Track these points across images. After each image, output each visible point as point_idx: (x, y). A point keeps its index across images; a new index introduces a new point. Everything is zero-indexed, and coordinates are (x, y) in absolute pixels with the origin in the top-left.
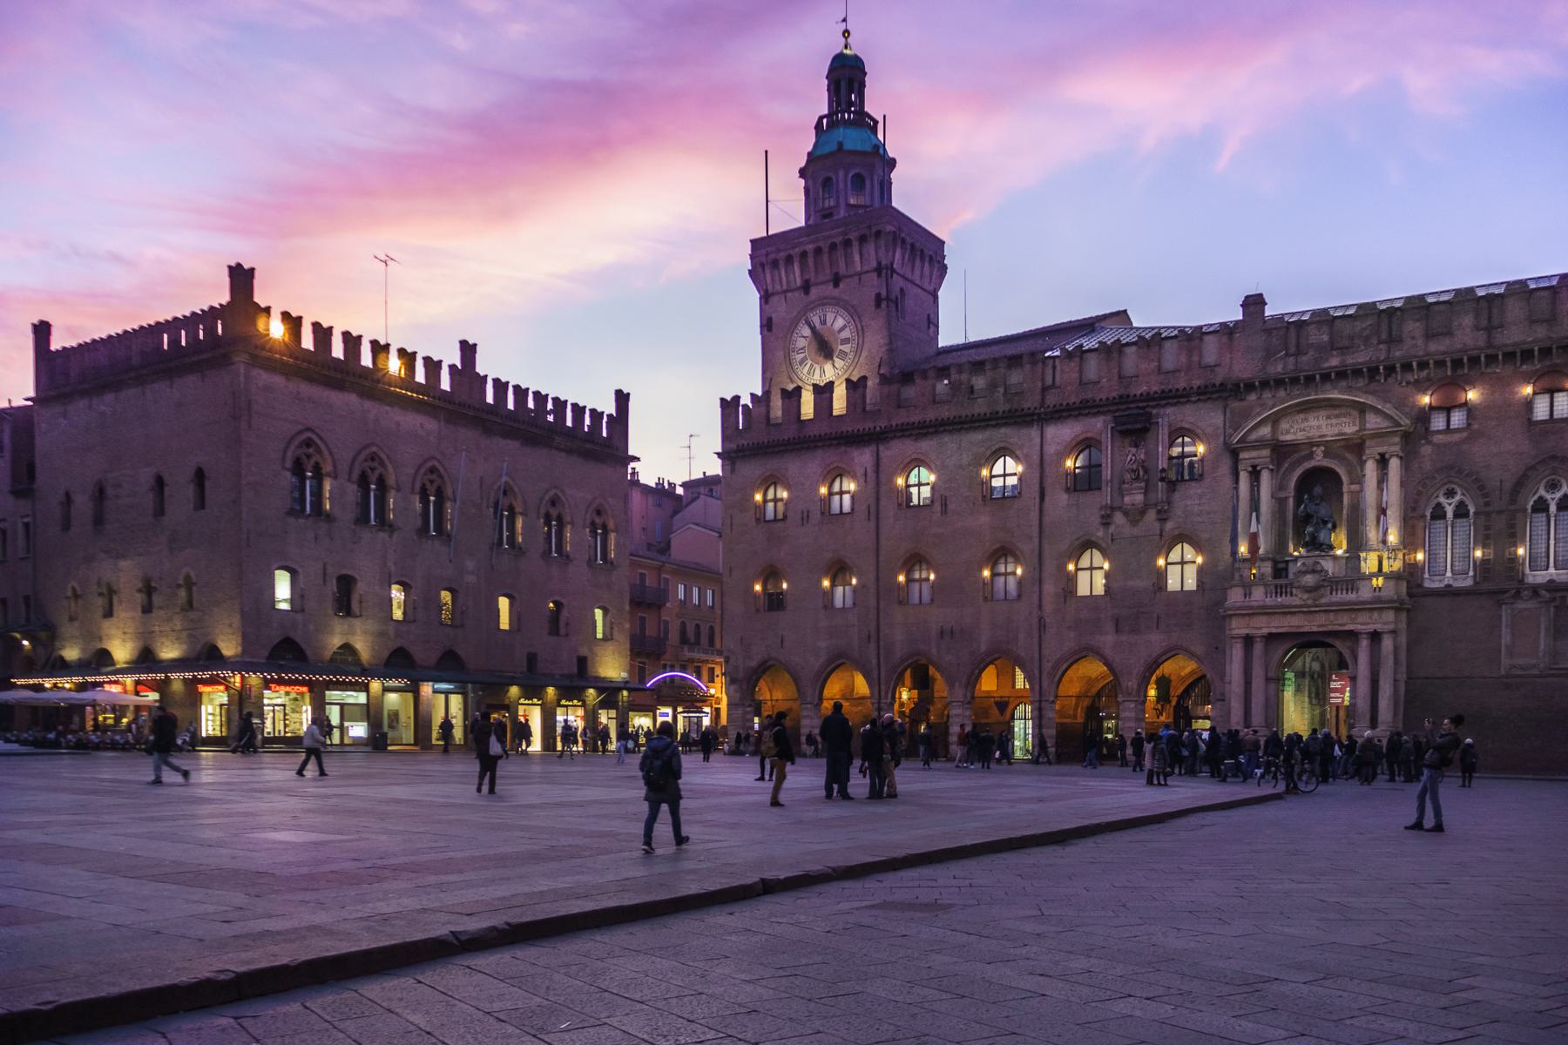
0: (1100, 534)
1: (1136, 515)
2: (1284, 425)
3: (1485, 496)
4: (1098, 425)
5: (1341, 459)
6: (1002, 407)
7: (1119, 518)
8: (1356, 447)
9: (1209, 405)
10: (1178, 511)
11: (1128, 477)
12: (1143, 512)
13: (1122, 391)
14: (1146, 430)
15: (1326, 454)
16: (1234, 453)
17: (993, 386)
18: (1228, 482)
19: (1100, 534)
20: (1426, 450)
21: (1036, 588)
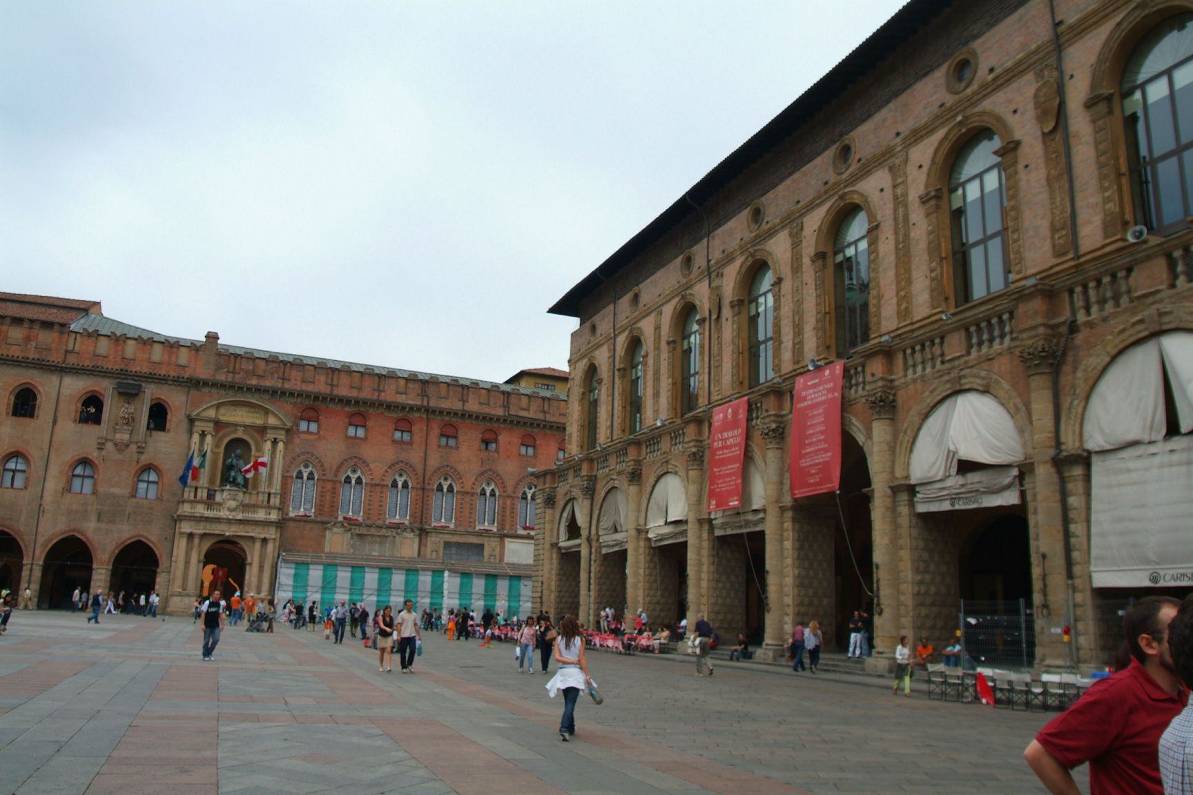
0: (95, 454)
1: (121, 447)
2: (222, 410)
5: (252, 438)
6: (32, 355)
8: (262, 430)
9: (179, 388)
11: (121, 422)
12: (127, 446)
13: (123, 367)
16: (191, 421)
17: (28, 339)
18: (185, 437)
20: (297, 441)
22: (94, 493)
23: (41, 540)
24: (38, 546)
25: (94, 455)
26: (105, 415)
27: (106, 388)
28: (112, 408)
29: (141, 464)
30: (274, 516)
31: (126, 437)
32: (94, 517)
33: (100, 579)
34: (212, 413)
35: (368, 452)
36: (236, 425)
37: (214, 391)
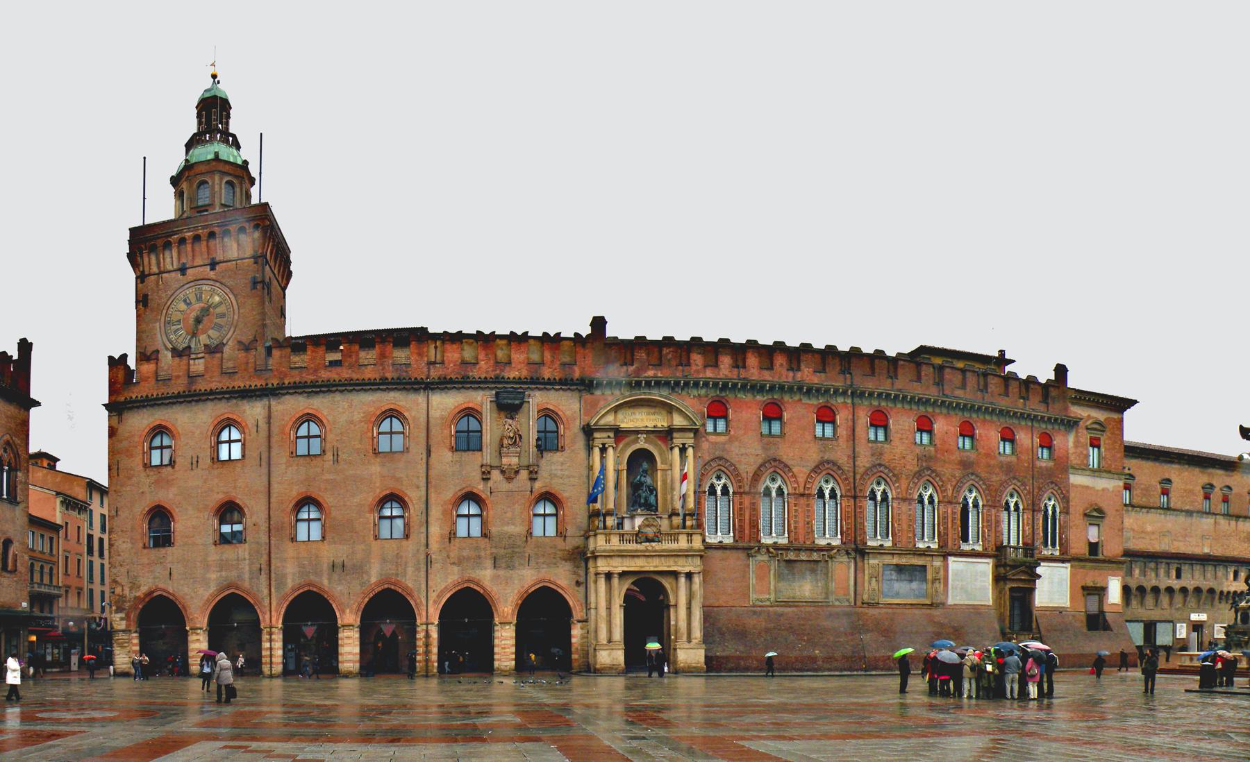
0: (481, 487)
1: (509, 474)
2: (620, 415)
3: (740, 481)
4: (482, 399)
5: (656, 445)
7: (496, 475)
8: (666, 435)
9: (569, 394)
10: (544, 473)
11: (505, 442)
12: (517, 472)
14: (520, 406)
15: (646, 441)
19: (481, 487)
20: (705, 445)
21: (424, 529)
22: (485, 535)
23: (433, 595)
24: (431, 602)
25: (480, 488)
26: (487, 438)
27: (482, 399)
28: (492, 427)
29: (536, 494)
30: (697, 543)
31: (515, 460)
32: (489, 563)
33: (505, 641)
34: (609, 419)
35: (786, 452)
36: (637, 432)
37: (608, 392)
